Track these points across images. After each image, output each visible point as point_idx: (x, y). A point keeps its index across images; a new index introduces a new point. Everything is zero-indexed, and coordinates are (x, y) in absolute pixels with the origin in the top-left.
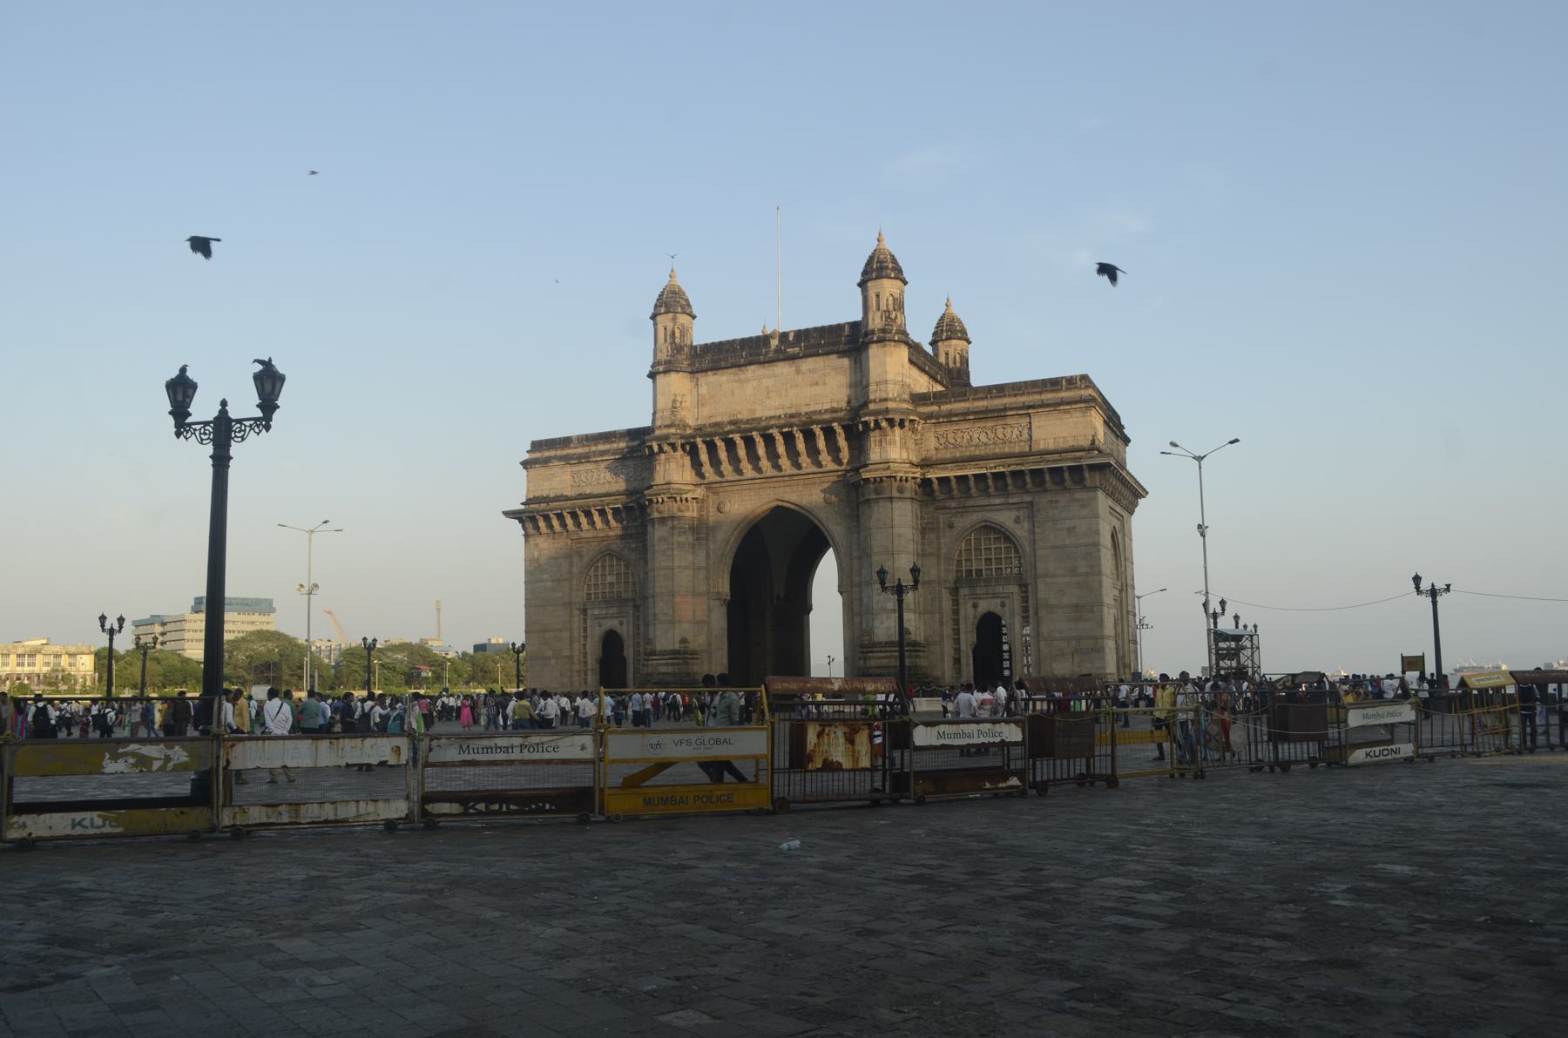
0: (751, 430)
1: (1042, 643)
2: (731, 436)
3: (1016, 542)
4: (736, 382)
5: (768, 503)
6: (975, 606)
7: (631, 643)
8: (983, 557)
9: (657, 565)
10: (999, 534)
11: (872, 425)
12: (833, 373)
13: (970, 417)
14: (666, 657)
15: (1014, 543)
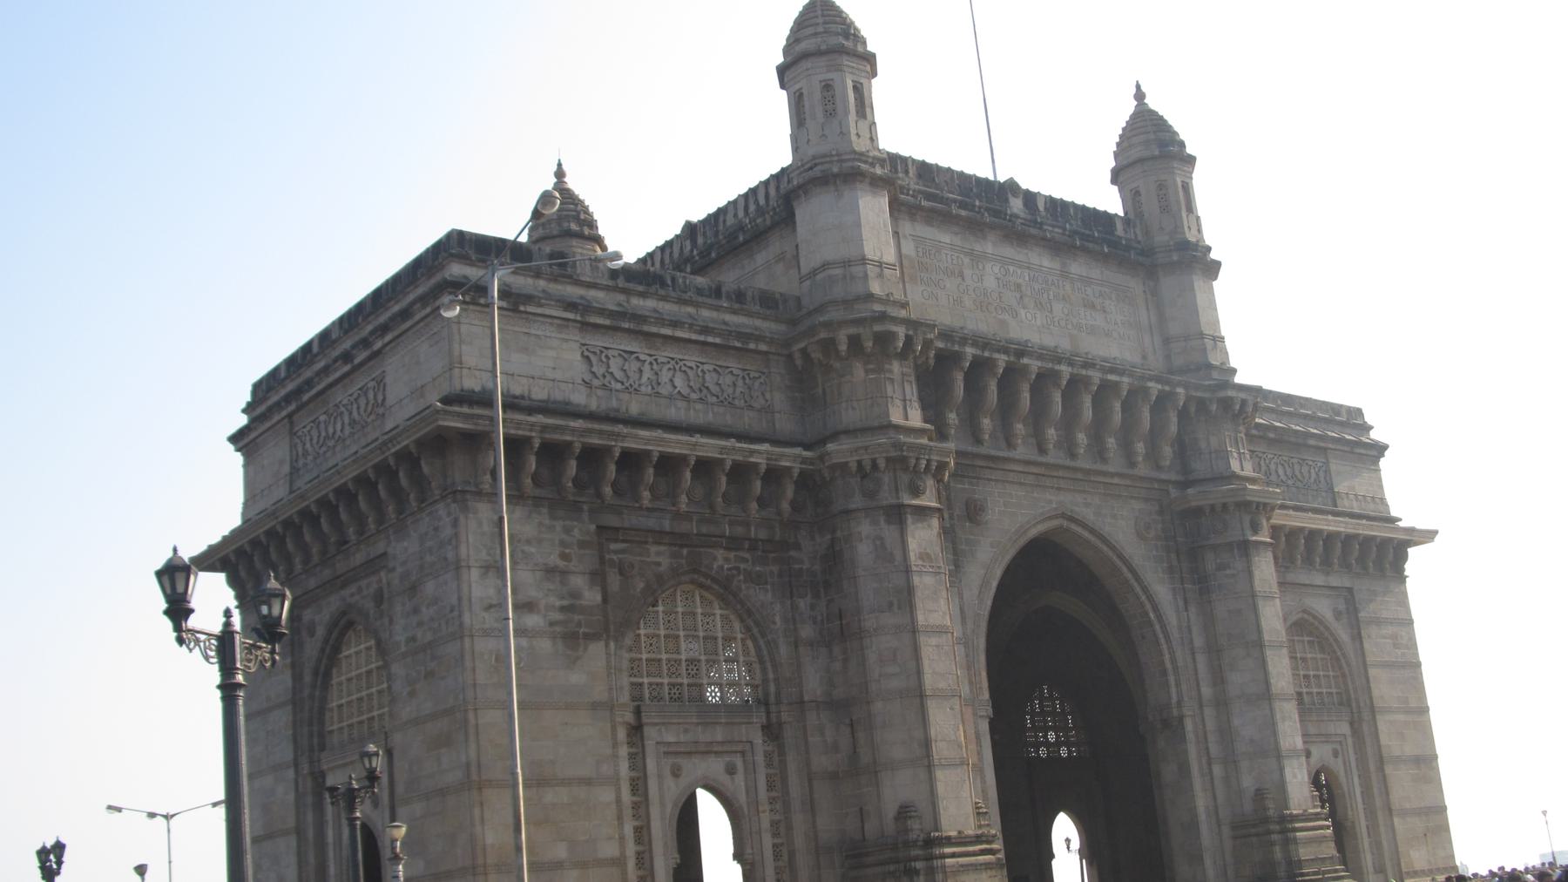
0: (1059, 360)
1: (1396, 820)
2: (1025, 361)
3: (1339, 653)
4: (966, 254)
5: (1050, 518)
6: (1308, 754)
7: (766, 819)
8: (1302, 673)
9: (921, 618)
10: (1310, 634)
11: (1238, 407)
12: (1113, 296)
13: (1272, 435)
14: (971, 849)
15: (1334, 652)
